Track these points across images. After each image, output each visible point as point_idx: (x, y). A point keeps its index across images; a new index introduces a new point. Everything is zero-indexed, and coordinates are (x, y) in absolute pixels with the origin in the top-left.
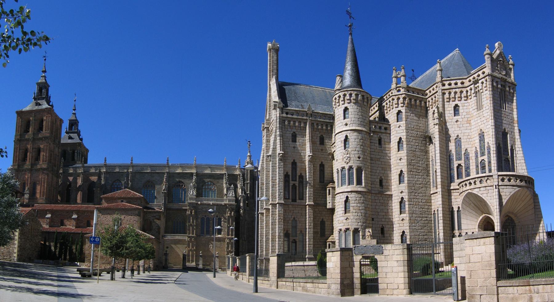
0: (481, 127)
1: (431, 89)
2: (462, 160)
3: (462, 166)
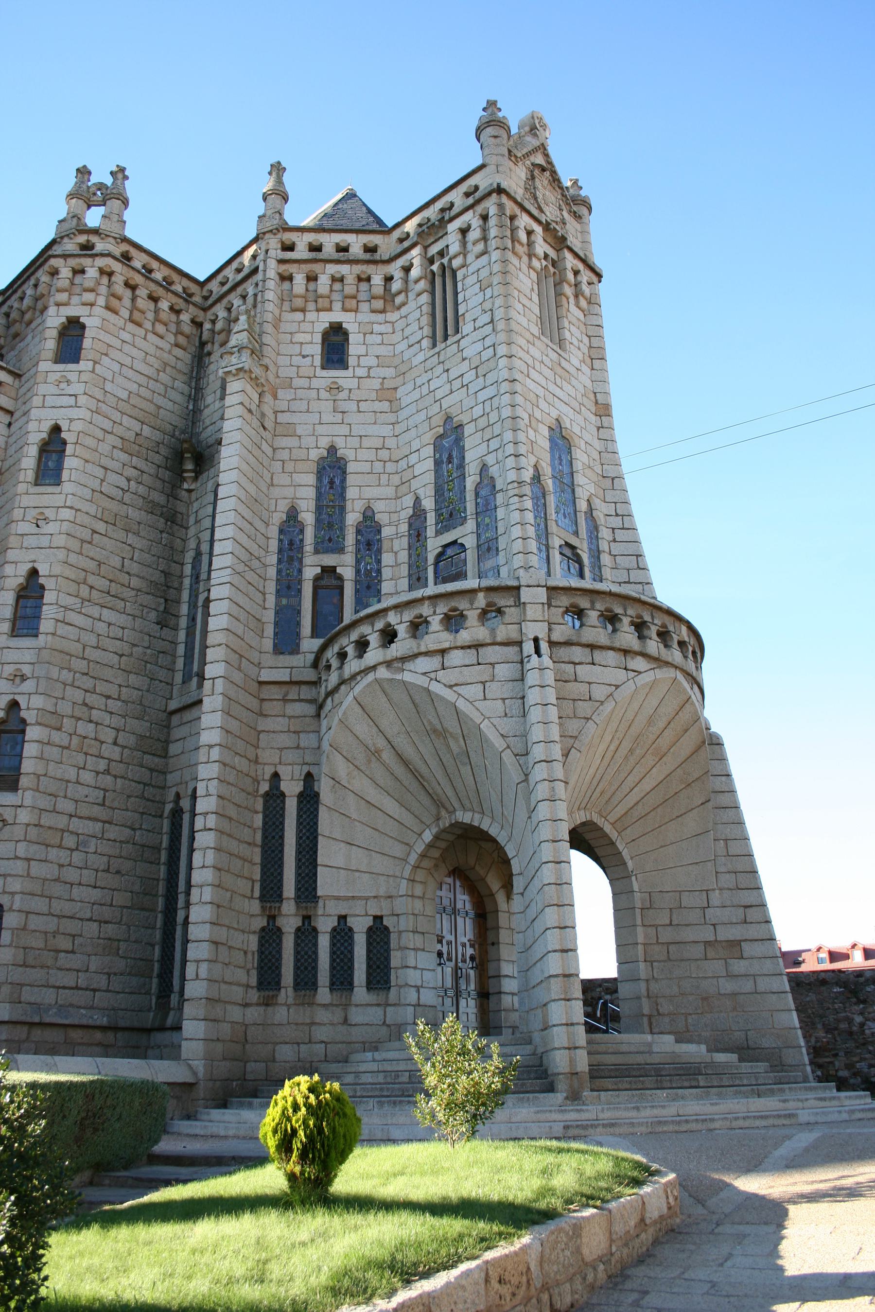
0: (445, 404)
1: (229, 272)
2: (341, 550)
3: (340, 578)
